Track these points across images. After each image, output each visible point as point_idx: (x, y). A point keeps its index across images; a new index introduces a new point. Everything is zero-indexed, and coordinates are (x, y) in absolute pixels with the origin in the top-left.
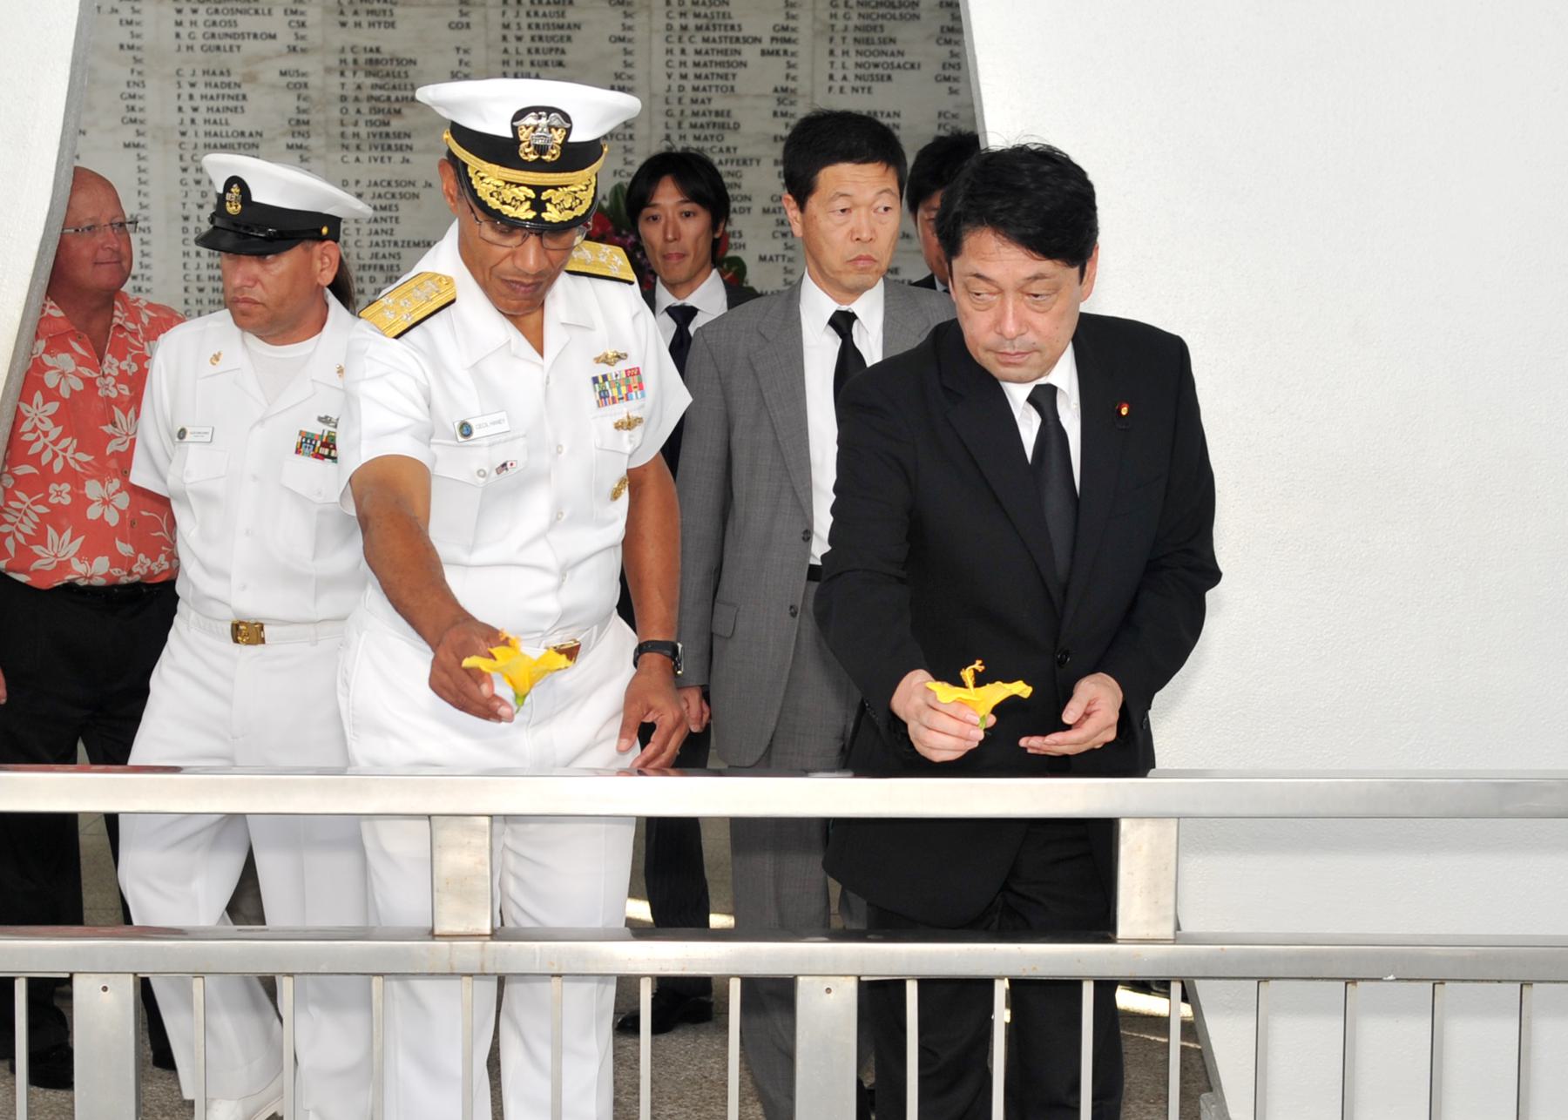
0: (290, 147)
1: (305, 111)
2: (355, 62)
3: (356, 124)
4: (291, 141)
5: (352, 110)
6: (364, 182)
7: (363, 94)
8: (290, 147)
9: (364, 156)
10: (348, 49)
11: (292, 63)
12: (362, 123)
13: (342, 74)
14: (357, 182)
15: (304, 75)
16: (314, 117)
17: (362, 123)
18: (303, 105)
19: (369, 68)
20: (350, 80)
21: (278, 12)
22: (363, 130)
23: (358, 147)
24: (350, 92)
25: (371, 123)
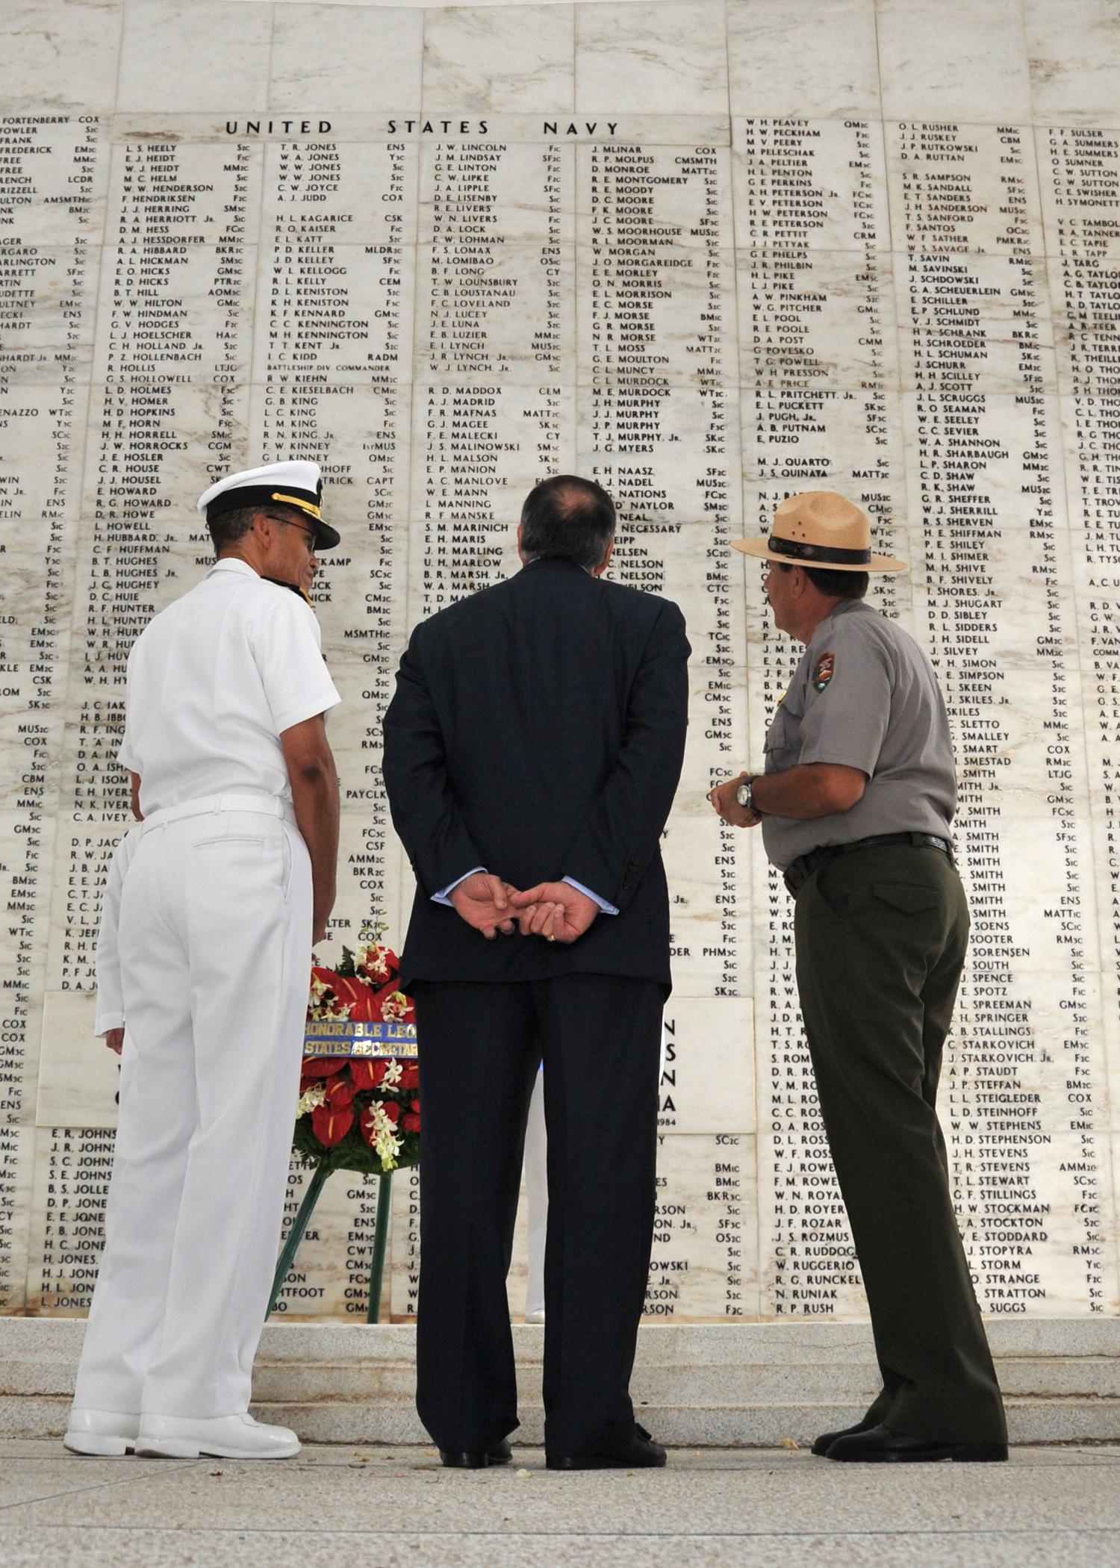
0: (20, 804)
1: (40, 768)
2: (97, 717)
3: (92, 781)
4: (23, 797)
5: (90, 766)
6: (95, 841)
7: (101, 751)
8: (20, 804)
9: (97, 814)
10: (91, 705)
11: (32, 718)
12: (98, 780)
13: (83, 729)
14: (88, 841)
15: (43, 730)
16: (49, 773)
17: (98, 780)
18: (39, 761)
19: (110, 723)
20: (90, 736)
21: (23, 668)
22: (99, 787)
23: (92, 805)
24: (89, 749)
25: (109, 780)
